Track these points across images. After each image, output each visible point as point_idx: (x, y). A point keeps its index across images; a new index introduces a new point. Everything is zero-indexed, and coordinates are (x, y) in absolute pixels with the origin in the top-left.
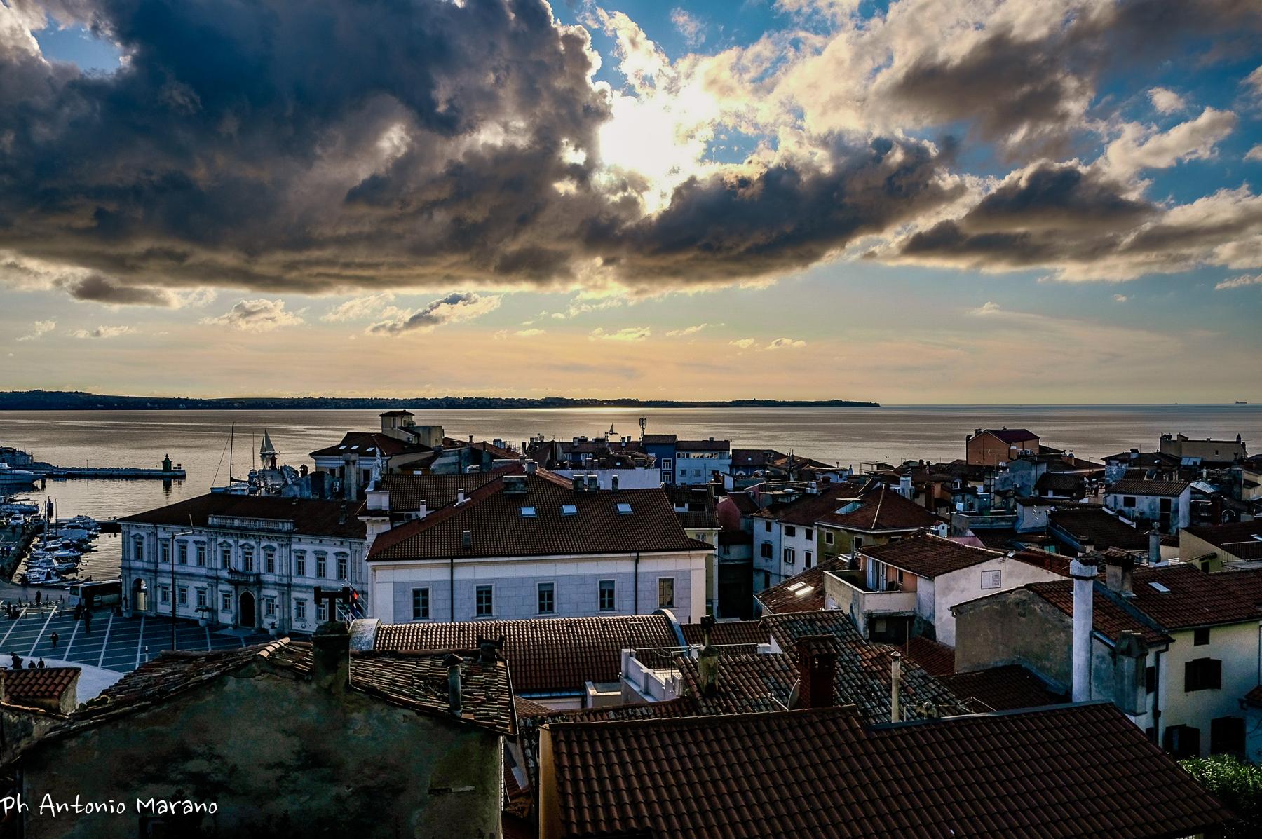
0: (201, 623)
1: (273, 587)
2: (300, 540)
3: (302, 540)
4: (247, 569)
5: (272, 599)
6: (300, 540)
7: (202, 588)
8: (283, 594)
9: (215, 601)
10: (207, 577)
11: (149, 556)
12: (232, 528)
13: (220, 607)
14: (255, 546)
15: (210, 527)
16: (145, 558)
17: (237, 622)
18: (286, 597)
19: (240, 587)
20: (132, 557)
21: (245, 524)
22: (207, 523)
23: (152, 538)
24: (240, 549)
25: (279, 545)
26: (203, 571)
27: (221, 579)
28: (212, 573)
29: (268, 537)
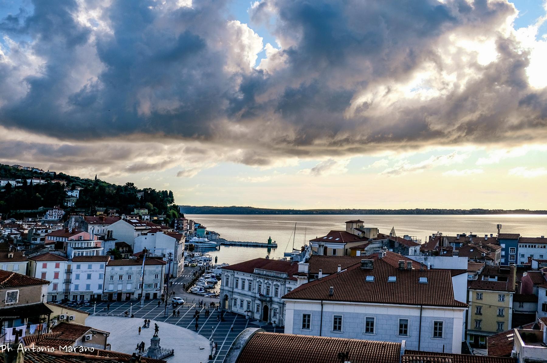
0: (247, 317)
1: (277, 304)
2: (289, 282)
3: (290, 283)
4: (267, 294)
5: (276, 309)
6: (289, 282)
7: (249, 301)
8: (280, 307)
9: (253, 308)
10: (251, 296)
11: (231, 285)
12: (262, 275)
13: (255, 311)
14: (271, 284)
15: (254, 274)
16: (229, 286)
17: (261, 318)
18: (282, 309)
19: (264, 302)
20: (224, 285)
21: (268, 273)
22: (253, 272)
23: (232, 277)
24: (265, 285)
25: (281, 284)
26: (250, 294)
27: (257, 298)
28: (253, 295)
29: (276, 280)
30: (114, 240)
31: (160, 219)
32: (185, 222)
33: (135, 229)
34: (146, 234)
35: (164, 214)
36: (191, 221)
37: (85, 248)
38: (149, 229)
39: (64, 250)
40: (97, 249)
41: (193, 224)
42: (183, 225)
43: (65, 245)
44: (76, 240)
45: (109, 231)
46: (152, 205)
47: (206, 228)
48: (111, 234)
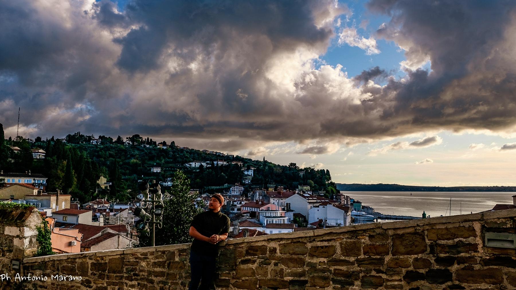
30: (292, 211)
31: (321, 194)
32: (342, 197)
33: (308, 202)
34: (318, 207)
35: (323, 191)
36: (347, 196)
37: (274, 217)
38: (319, 202)
39: (257, 219)
40: (284, 218)
41: (349, 199)
42: (340, 200)
43: (257, 214)
44: (265, 211)
45: (287, 204)
46: (313, 182)
47: (361, 203)
48: (289, 206)
